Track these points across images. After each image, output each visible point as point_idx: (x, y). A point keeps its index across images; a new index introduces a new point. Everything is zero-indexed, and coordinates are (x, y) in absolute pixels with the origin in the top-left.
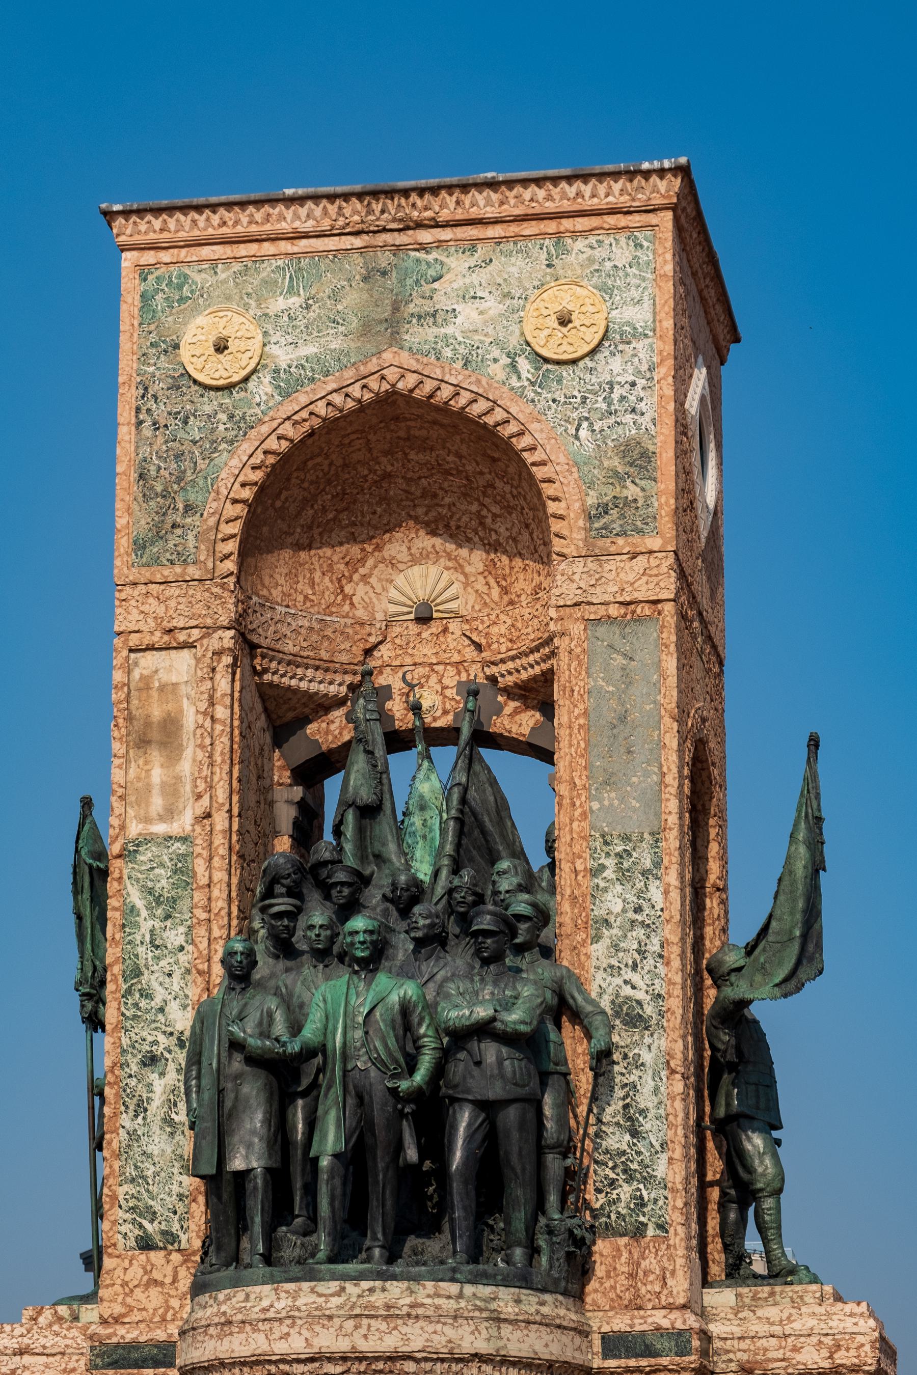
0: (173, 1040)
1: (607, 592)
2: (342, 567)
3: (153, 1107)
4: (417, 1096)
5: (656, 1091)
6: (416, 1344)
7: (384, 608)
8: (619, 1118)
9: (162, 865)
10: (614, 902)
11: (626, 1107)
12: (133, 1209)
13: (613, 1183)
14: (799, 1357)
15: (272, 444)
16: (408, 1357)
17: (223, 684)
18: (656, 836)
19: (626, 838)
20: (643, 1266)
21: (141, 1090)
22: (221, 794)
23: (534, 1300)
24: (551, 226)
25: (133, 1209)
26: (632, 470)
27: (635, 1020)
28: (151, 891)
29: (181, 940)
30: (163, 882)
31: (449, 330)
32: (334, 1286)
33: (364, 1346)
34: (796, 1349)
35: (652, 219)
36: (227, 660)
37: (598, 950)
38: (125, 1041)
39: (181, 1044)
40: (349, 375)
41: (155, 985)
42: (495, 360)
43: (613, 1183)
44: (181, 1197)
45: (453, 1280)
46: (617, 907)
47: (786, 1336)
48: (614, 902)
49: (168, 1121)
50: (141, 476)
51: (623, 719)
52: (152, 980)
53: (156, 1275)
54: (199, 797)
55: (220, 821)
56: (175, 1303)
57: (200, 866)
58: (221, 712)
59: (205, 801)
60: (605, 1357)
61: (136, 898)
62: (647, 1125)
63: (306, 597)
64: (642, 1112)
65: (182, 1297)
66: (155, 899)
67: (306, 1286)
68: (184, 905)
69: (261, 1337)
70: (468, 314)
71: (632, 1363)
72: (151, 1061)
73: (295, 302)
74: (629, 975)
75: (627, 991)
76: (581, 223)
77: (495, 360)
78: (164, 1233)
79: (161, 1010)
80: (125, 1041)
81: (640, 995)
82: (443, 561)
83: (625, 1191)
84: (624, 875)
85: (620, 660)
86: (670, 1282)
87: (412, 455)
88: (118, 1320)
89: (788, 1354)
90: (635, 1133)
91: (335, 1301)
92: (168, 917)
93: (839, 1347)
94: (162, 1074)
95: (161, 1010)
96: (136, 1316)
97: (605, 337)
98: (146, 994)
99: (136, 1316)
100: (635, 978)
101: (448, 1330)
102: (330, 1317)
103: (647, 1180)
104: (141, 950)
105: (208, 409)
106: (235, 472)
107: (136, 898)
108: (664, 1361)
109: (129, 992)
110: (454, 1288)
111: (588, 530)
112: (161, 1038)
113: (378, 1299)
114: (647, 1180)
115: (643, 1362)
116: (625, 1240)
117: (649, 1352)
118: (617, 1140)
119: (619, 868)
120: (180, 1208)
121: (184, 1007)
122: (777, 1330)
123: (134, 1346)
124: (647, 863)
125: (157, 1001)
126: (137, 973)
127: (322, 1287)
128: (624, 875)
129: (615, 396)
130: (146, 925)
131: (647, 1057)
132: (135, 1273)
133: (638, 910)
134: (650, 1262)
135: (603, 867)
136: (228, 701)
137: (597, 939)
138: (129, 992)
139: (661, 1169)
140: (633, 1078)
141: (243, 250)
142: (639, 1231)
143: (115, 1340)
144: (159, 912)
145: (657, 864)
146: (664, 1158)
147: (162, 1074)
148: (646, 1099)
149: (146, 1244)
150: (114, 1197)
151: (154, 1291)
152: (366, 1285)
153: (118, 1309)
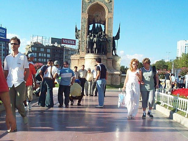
27: (110, 41)
55: (87, 28)
72: (83, 41)
118: (109, 47)
148: (110, 45)
149: (82, 51)
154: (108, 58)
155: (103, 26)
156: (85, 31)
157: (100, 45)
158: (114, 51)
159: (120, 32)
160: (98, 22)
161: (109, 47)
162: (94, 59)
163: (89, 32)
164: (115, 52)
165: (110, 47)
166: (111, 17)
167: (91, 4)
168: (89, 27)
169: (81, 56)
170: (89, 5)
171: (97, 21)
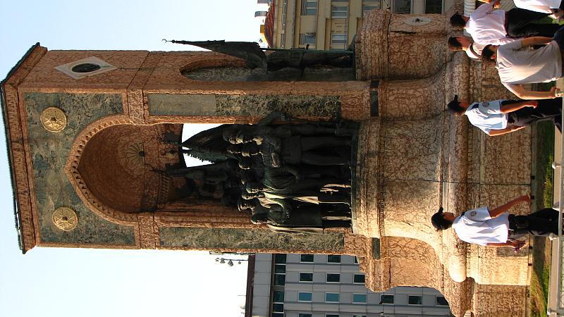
2: (129, 178)
7: (140, 166)
8: (305, 109)
9: (227, 237)
11: (301, 107)
13: (325, 111)
14: (378, 53)
15: (96, 204)
16: (378, 181)
17: (171, 219)
18: (217, 96)
20: (350, 103)
22: (206, 220)
23: (361, 141)
24: (23, 123)
26: (101, 100)
27: (273, 105)
33: (375, 195)
34: (376, 54)
35: (20, 94)
36: (163, 218)
37: (252, 114)
41: (264, 239)
42: (67, 140)
44: (328, 233)
47: (371, 58)
51: (180, 105)
52: (262, 240)
55: (214, 220)
58: (180, 220)
59: (208, 225)
62: (306, 101)
63: (139, 190)
64: (303, 102)
66: (238, 239)
69: (372, 221)
70: (52, 147)
71: (380, 108)
72: (287, 240)
74: (260, 105)
75: (265, 106)
76: (22, 114)
77: (67, 140)
78: (339, 238)
79: (271, 238)
81: (266, 102)
82: (126, 148)
83: (327, 108)
87: (94, 159)
89: (377, 57)
90: (309, 105)
91: (362, 201)
93: (375, 42)
95: (271, 238)
97: (59, 108)
98: (267, 242)
101: (371, 170)
102: (367, 203)
103: (324, 101)
104: (253, 243)
105: (85, 223)
106: (105, 218)
108: (379, 99)
111: (121, 114)
112: (280, 237)
114: (324, 101)
116: (342, 109)
118: (311, 109)
119: (228, 106)
120: (332, 233)
126: (261, 244)
131: (286, 100)
133: (240, 102)
134: (349, 101)
136: (176, 218)
140: (292, 105)
141: (34, 212)
142: (339, 104)
144: (242, 237)
147: (291, 238)
148: (299, 101)
149: (342, 243)
154: (374, 113)
156: (228, 231)
157: (301, 167)
159: (218, 39)
160: (172, 152)
161: (311, 109)
162: (380, 208)
165: (309, 105)
167: (87, 205)
170: (90, 214)
171: (170, 156)
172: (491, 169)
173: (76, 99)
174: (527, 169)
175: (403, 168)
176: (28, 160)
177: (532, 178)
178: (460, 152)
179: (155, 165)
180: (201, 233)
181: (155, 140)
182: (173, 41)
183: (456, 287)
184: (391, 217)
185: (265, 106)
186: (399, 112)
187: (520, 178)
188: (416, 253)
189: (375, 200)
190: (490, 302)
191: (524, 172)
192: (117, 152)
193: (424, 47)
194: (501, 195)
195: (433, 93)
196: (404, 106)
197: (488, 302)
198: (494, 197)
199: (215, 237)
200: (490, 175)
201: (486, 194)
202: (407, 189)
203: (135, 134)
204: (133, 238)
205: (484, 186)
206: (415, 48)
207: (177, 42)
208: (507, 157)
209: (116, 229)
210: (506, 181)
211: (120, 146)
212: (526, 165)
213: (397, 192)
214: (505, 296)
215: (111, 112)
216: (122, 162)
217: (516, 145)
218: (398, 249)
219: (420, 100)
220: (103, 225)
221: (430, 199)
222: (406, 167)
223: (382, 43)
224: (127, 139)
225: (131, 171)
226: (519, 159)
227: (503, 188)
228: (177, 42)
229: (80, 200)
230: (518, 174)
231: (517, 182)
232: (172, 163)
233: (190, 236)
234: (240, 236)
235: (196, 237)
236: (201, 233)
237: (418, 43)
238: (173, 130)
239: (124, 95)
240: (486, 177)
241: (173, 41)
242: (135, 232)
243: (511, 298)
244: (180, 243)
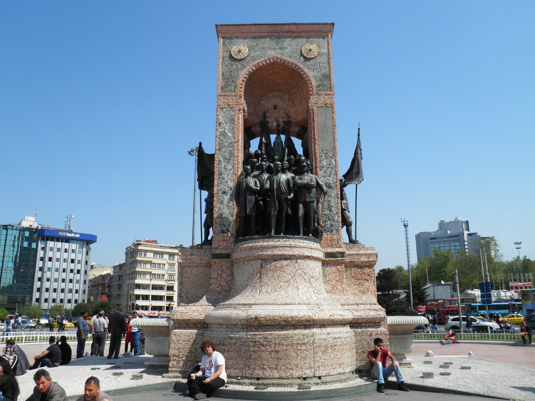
0: (229, 189)
1: (320, 102)
3: (224, 203)
4: (291, 198)
5: (335, 202)
6: (296, 253)
10: (324, 163)
12: (220, 224)
13: (326, 221)
16: (294, 256)
19: (327, 150)
21: (222, 199)
25: (220, 224)
27: (329, 187)
28: (224, 157)
29: (231, 168)
30: (227, 156)
31: (286, 51)
32: (277, 240)
38: (218, 189)
39: (231, 189)
40: (266, 58)
43: (326, 221)
45: (302, 239)
46: (325, 164)
47: (359, 255)
48: (324, 163)
49: (229, 206)
50: (223, 75)
52: (224, 176)
53: (225, 238)
54: (235, 138)
56: (229, 245)
57: (235, 152)
60: (326, 258)
61: (221, 159)
65: (231, 244)
66: (224, 158)
67: (270, 240)
68: (232, 160)
71: (332, 259)
72: (224, 193)
73: (255, 44)
74: (328, 178)
75: (328, 181)
80: (218, 189)
81: (331, 182)
83: (329, 223)
84: (326, 157)
85: (324, 115)
86: (339, 242)
88: (216, 248)
90: (330, 211)
91: (278, 243)
92: (228, 163)
94: (227, 196)
96: (221, 247)
98: (223, 179)
99: (221, 247)
100: (330, 179)
102: (277, 247)
103: (333, 220)
106: (243, 74)
107: (221, 159)
108: (339, 259)
109: (219, 178)
110: (302, 241)
112: (226, 188)
113: (288, 243)
114: (333, 220)
115: (334, 259)
117: (336, 257)
121: (231, 182)
122: (357, 253)
123: (221, 254)
124: (331, 155)
125: (226, 180)
126: (221, 174)
127: (274, 240)
128: (326, 157)
129: (321, 65)
130: (223, 165)
131: (333, 195)
132: (221, 238)
133: (330, 165)
135: (322, 156)
137: (321, 170)
138: (219, 178)
139: (336, 218)
142: (332, 231)
143: (216, 253)
145: (333, 155)
146: (337, 216)
147: (227, 196)
148: (332, 203)
149: (223, 232)
150: (216, 222)
151: (225, 242)
152: (284, 240)
153: (217, 246)
155: (297, 143)
158: (345, 227)
163: (248, 158)
164: (349, 232)
165: (330, 211)
166: (328, 101)
168: (247, 146)
169: (218, 251)
170: (244, 67)
171: (275, 124)
172: (325, 344)
173: (325, 64)
174: (326, 372)
175: (304, 274)
176: (282, 34)
177: (320, 378)
178: (333, 318)
179: (267, 114)
180: (230, 135)
181: (285, 115)
182: (359, 129)
183: (200, 316)
184: (263, 266)
185: (328, 181)
186: (329, 273)
187: (319, 368)
188: (217, 286)
189: (280, 253)
190: (188, 342)
191: (323, 370)
192: (277, 92)
193: (368, 290)
194: (306, 353)
195: (348, 297)
196: (334, 276)
197: (187, 341)
198: (304, 347)
199: (227, 144)
200: (320, 343)
201: (306, 341)
202: (290, 277)
203: (291, 104)
204: (226, 91)
205: (312, 339)
206: (367, 284)
207: (359, 131)
208: (332, 356)
209: (232, 82)
210: (316, 356)
211: (281, 94)
212: (328, 371)
213: (286, 270)
214: (193, 354)
215: (317, 84)
216: (270, 95)
217: (339, 362)
218: (219, 272)
219: (339, 287)
220: (235, 74)
221: (285, 295)
222: (305, 277)
223: (369, 261)
224: (287, 98)
225: (263, 100)
226: (332, 365)
227: (311, 354)
228: (359, 131)
229: (253, 61)
230: (322, 366)
231: (316, 365)
232: (270, 125)
233: (227, 128)
234: (228, 160)
235: (226, 131)
236: (230, 135)
237: (371, 286)
238: (293, 127)
239: (330, 93)
240: (319, 340)
241: (359, 129)
242: (231, 93)
243: (191, 359)
244: (221, 120)
